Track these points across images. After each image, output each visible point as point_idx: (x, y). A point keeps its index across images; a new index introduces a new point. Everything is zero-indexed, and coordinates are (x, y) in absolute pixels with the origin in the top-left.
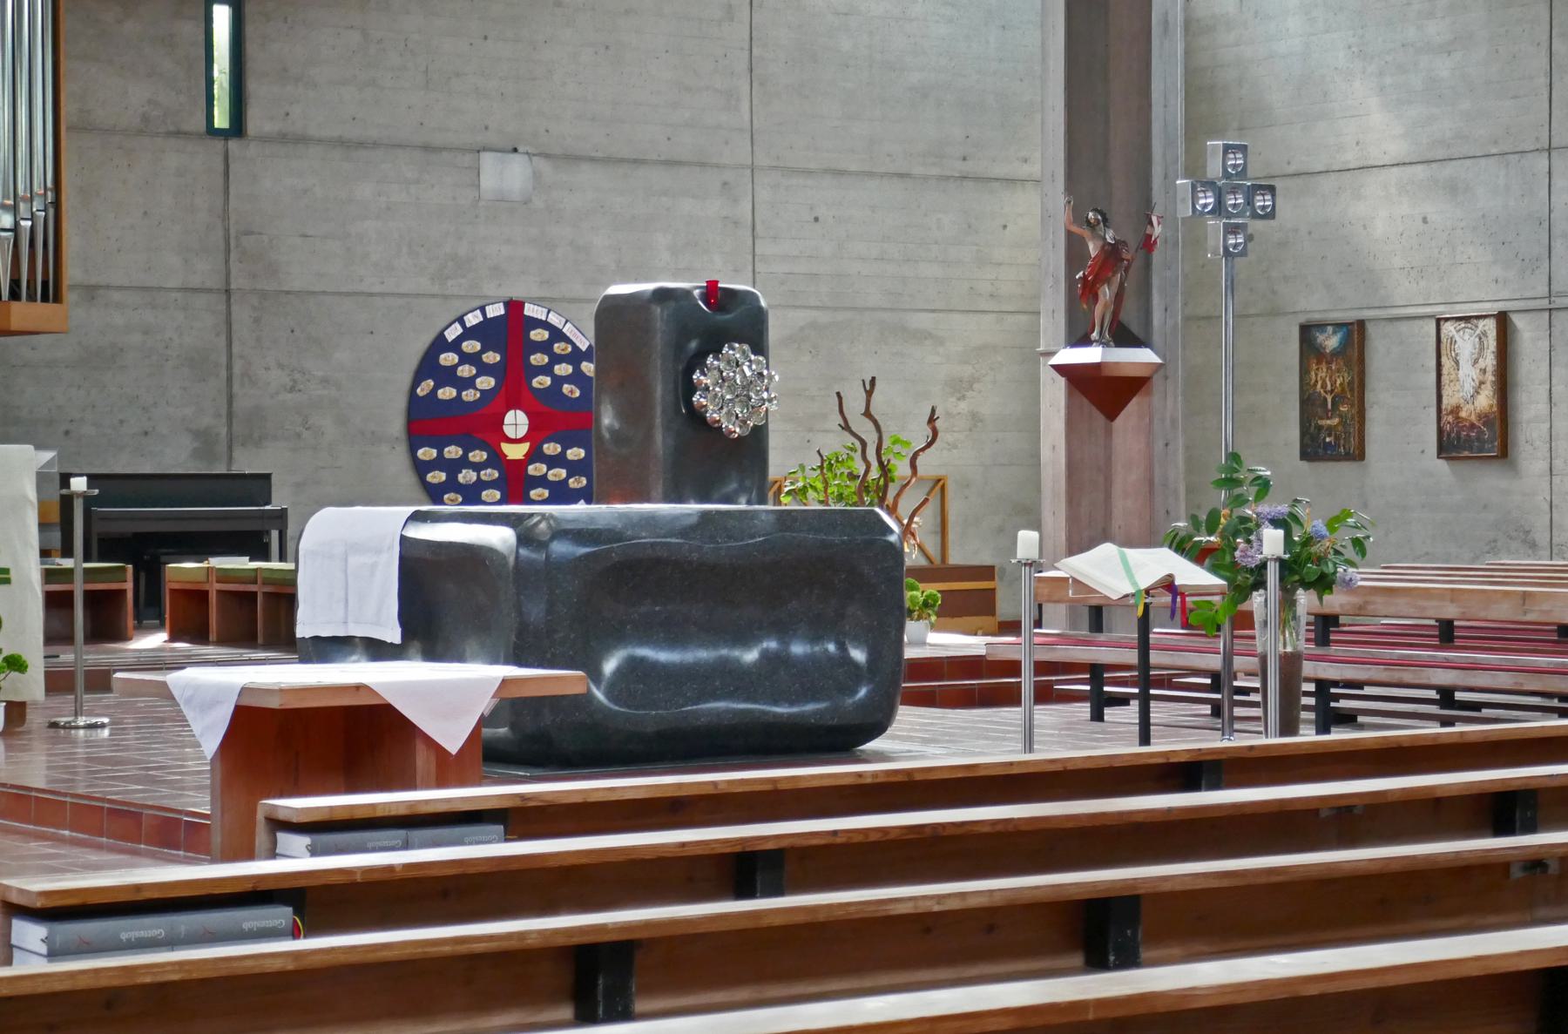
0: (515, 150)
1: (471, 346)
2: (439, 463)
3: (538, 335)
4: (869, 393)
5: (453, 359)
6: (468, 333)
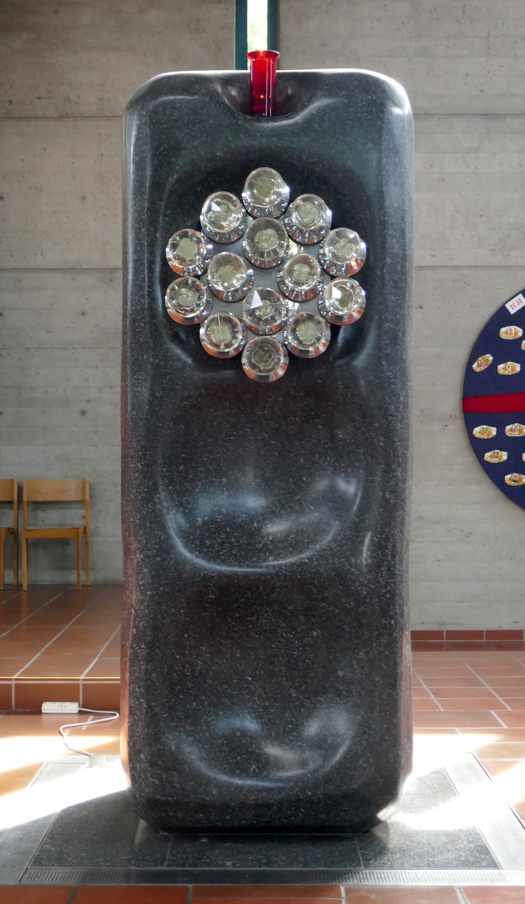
5: (516, 333)
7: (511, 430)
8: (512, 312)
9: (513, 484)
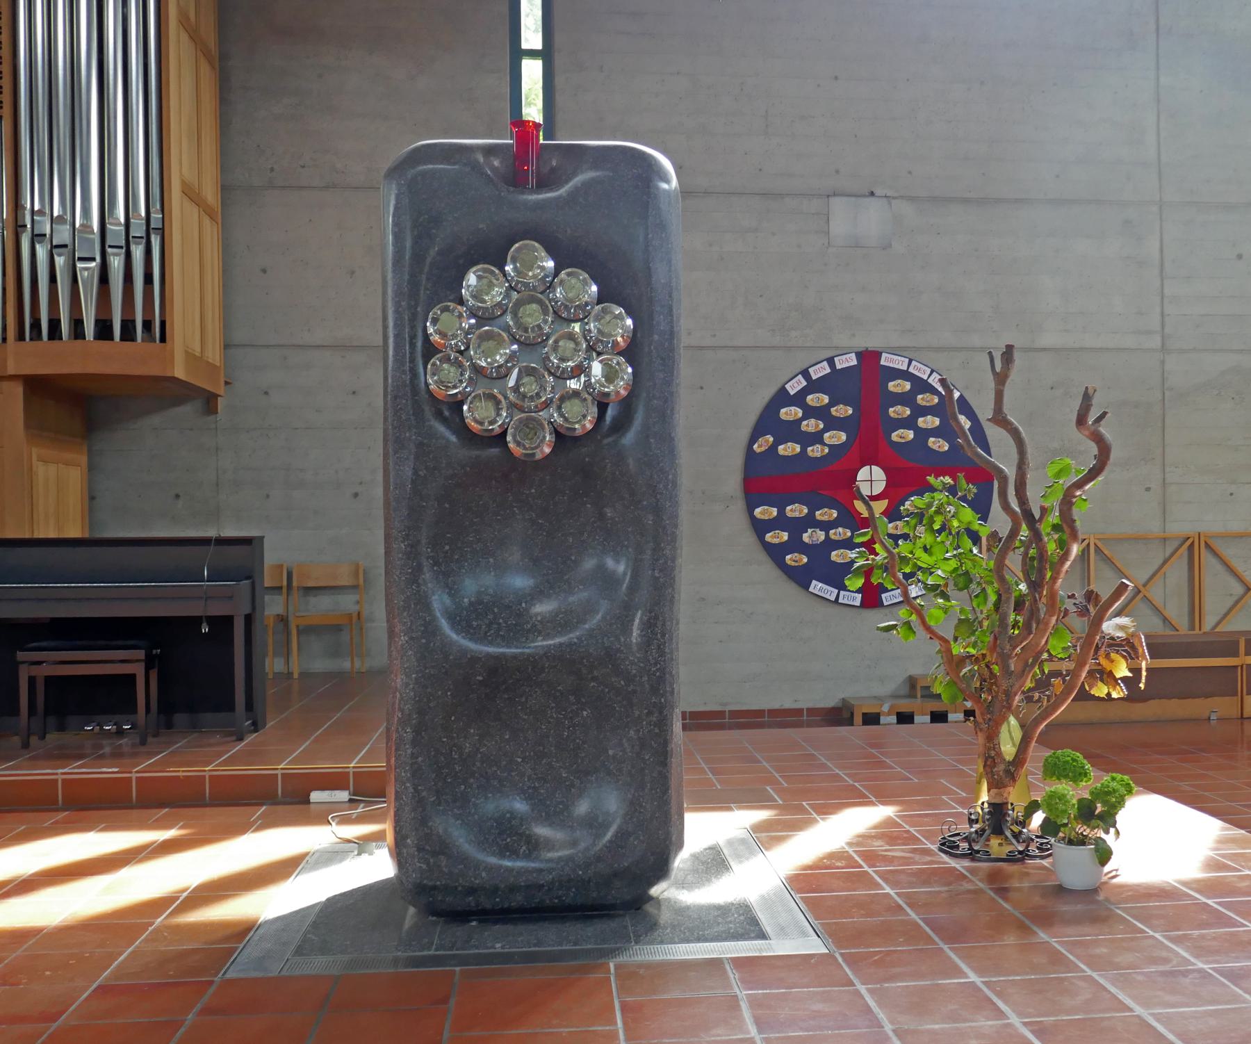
0: (872, 194)
1: (817, 399)
2: (780, 522)
3: (898, 386)
4: (1001, 379)
5: (796, 414)
6: (814, 386)
7: (791, 510)
8: (792, 393)
9: (793, 564)
